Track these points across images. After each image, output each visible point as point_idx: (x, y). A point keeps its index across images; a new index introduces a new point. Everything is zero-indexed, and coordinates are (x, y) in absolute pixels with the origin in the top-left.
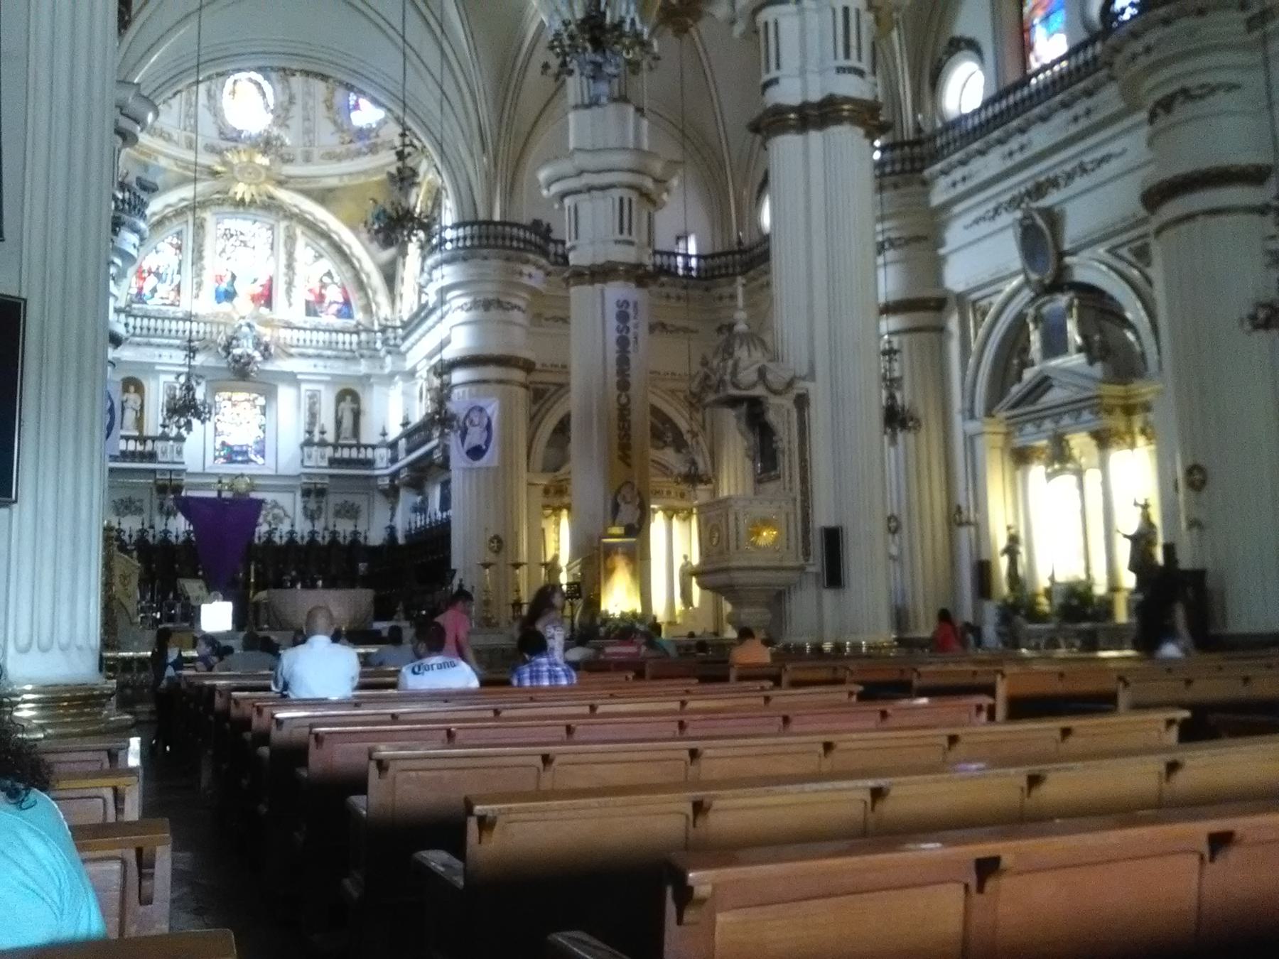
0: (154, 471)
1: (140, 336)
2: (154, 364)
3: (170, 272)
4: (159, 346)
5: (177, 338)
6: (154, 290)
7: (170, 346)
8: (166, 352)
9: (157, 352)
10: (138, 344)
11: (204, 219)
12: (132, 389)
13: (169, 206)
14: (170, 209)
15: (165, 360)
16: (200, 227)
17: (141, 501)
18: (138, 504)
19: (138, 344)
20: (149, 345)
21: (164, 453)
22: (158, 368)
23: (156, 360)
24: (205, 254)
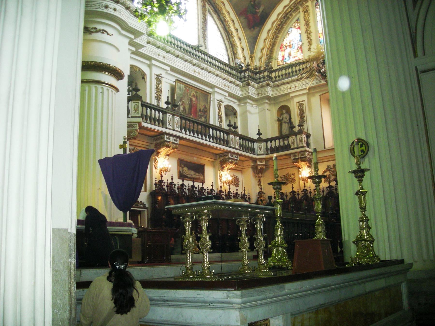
0: (290, 154)
1: (279, 80)
2: (288, 94)
3: (296, 42)
4: (288, 83)
5: (296, 75)
6: (290, 54)
7: (293, 81)
8: (293, 85)
9: (288, 86)
10: (278, 86)
11: (307, 6)
12: (284, 111)
13: (285, 7)
14: (287, 8)
15: (293, 89)
16: (306, 11)
17: (293, 174)
18: (293, 176)
19: (278, 86)
20: (283, 84)
21: (293, 143)
22: (291, 95)
23: (289, 91)
24: (311, 24)
